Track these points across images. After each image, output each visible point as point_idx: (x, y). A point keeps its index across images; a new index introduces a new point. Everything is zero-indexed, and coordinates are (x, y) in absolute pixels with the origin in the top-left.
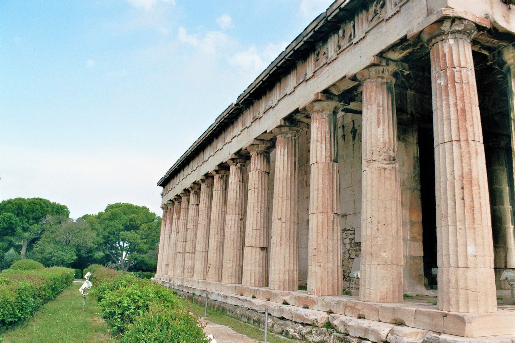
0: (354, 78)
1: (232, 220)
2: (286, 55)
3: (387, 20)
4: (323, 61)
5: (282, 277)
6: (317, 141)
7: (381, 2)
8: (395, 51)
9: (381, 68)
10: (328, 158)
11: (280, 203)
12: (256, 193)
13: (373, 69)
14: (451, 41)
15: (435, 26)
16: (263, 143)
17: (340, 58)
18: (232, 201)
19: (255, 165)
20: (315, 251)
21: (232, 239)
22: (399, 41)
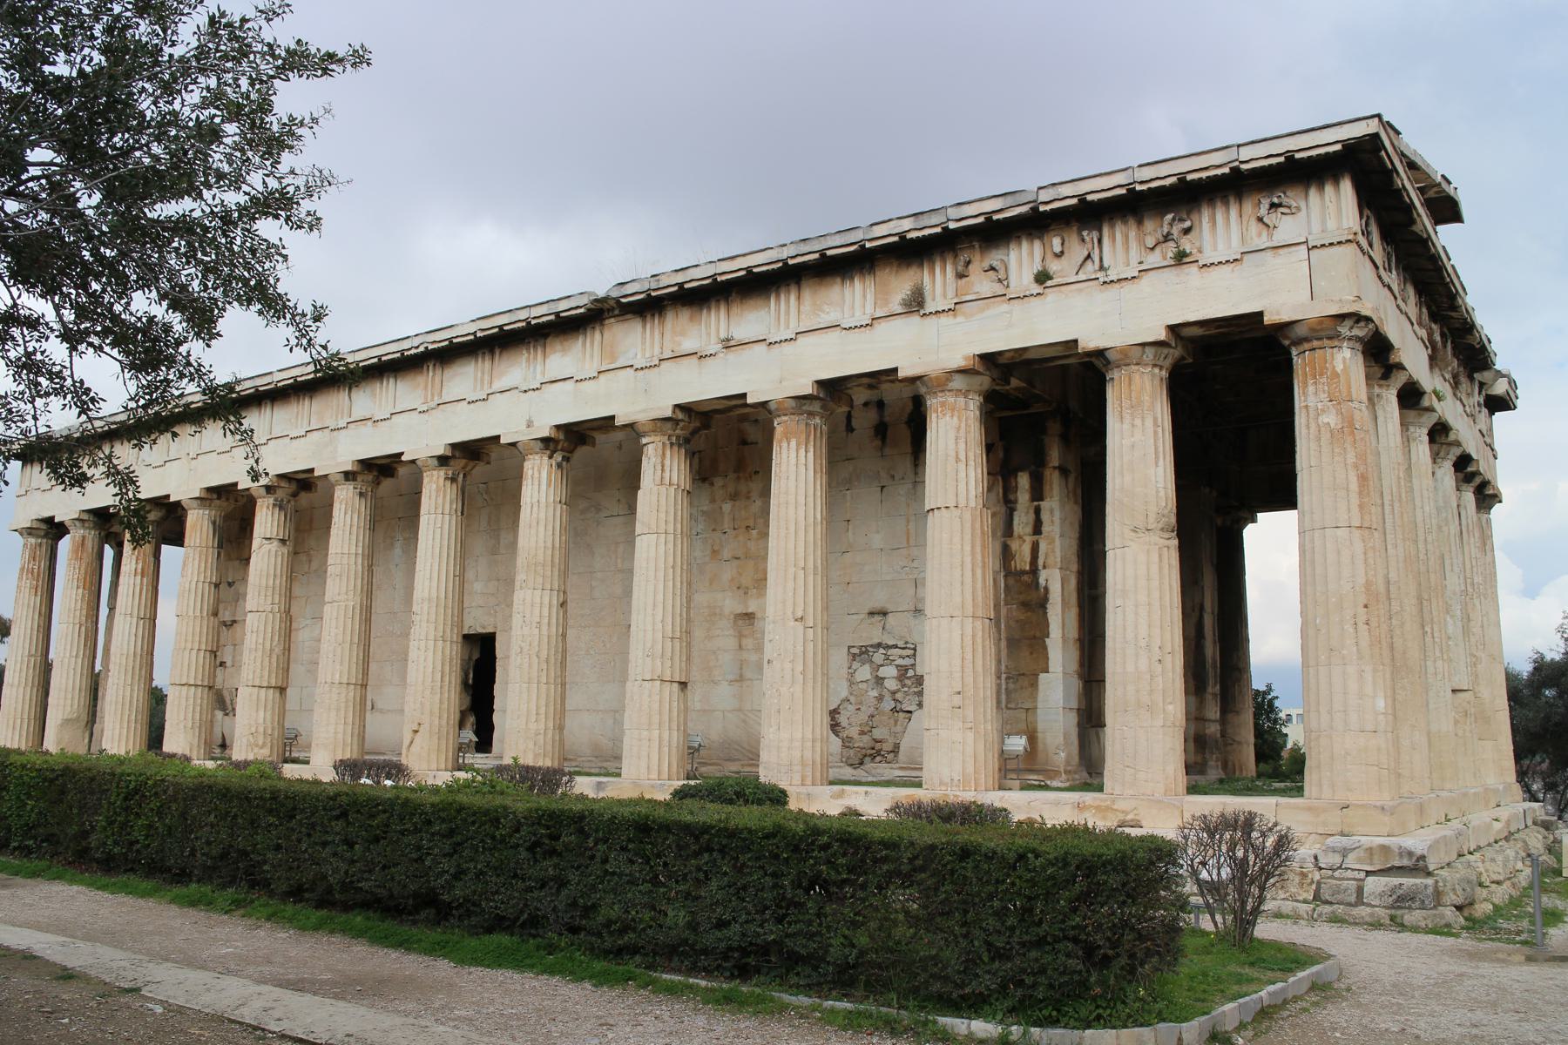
0: (1100, 353)
4: (982, 284)
5: (808, 754)
6: (958, 460)
7: (1187, 224)
9: (1166, 351)
11: (801, 582)
12: (671, 546)
13: (1150, 351)
14: (1347, 353)
15: (1328, 323)
18: (541, 552)
20: (957, 700)
21: (544, 654)
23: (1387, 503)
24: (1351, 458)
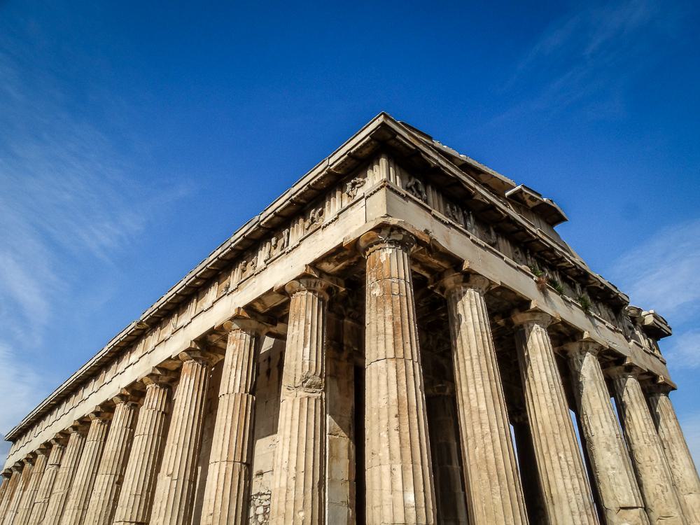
1: (103, 481)
2: (209, 264)
3: (324, 227)
4: (250, 271)
7: (320, 209)
8: (330, 263)
9: (314, 281)
10: (243, 390)
12: (145, 441)
15: (374, 233)
16: (166, 373)
17: (270, 267)
19: (149, 401)
22: (334, 250)
23: (474, 357)
24: (389, 313)
